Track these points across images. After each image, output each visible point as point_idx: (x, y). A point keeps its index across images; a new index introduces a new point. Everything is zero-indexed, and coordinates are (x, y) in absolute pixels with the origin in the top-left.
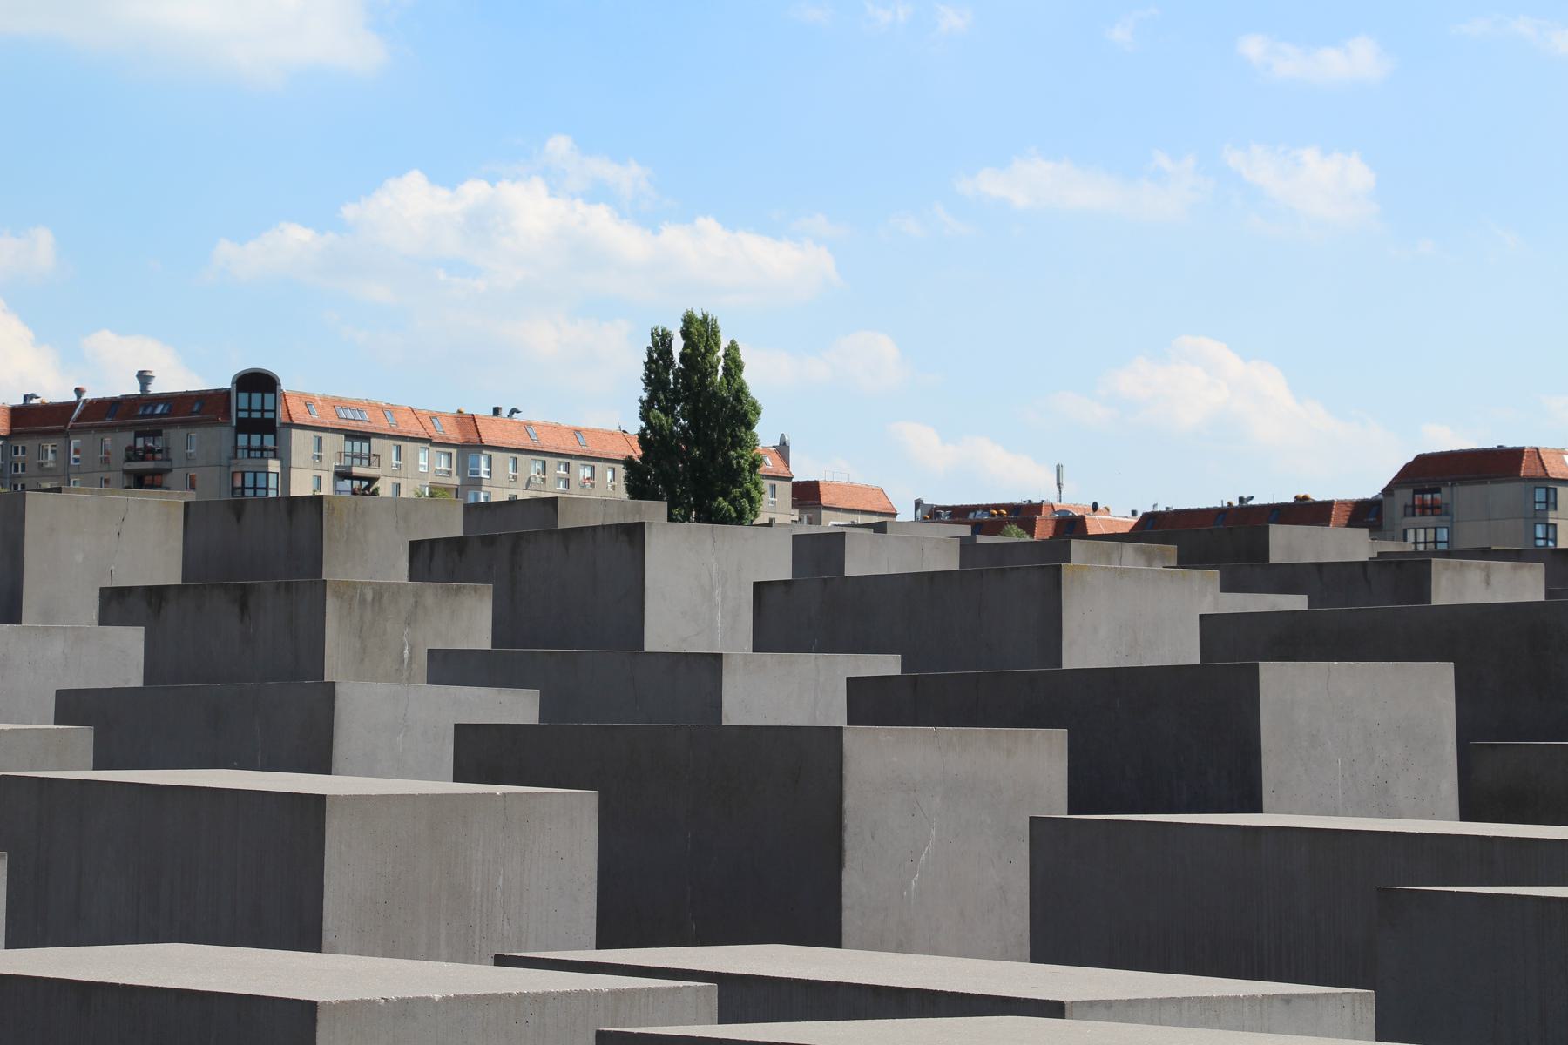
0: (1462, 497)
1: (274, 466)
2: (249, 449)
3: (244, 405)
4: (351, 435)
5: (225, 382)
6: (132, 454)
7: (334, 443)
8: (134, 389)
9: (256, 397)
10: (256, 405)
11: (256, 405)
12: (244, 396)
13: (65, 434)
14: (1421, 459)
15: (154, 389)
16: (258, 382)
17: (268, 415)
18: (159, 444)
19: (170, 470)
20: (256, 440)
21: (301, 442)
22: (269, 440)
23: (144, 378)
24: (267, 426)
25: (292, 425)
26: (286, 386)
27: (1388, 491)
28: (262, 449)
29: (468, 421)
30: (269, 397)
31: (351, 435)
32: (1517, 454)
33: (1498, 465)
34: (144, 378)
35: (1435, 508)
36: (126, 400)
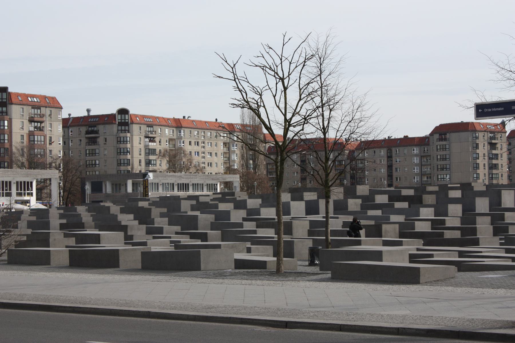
0: (453, 136)
1: (129, 135)
2: (122, 130)
3: (119, 118)
5: (114, 111)
6: (87, 133)
7: (144, 128)
8: (86, 114)
9: (123, 116)
10: (123, 118)
11: (123, 118)
12: (119, 116)
14: (441, 126)
15: (92, 114)
16: (123, 112)
17: (127, 121)
18: (95, 129)
19: (99, 137)
20: (123, 128)
21: (135, 128)
22: (127, 128)
23: (88, 111)
24: (126, 124)
25: (132, 123)
26: (131, 112)
28: (125, 130)
30: (127, 116)
31: (149, 126)
34: (88, 111)
35: (445, 139)
36: (85, 117)
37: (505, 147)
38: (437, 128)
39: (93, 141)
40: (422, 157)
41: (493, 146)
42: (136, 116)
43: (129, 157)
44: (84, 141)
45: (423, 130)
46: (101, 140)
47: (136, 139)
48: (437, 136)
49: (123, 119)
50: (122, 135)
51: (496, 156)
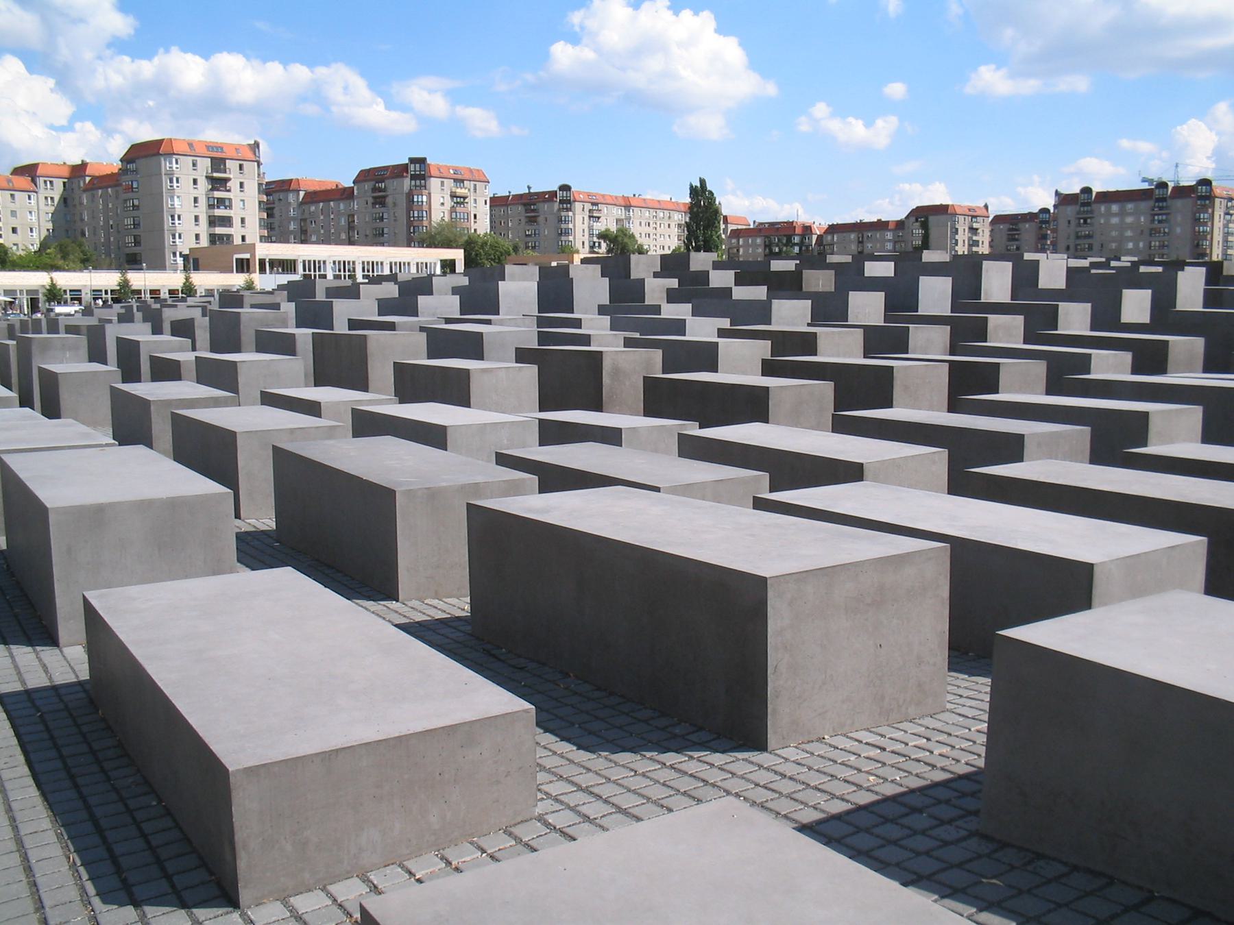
1: (570, 214)
4: (593, 204)
13: (507, 205)
16: (565, 188)
24: (569, 202)
27: (907, 217)
29: (626, 199)
31: (593, 204)
32: (947, 206)
33: (942, 210)
34: (529, 188)
37: (987, 233)
38: (913, 211)
39: (532, 220)
40: (895, 242)
41: (973, 231)
42: (579, 193)
43: (571, 238)
44: (523, 220)
45: (895, 211)
46: (541, 219)
47: (579, 219)
48: (913, 219)
49: (563, 197)
50: (563, 214)
51: (976, 243)
